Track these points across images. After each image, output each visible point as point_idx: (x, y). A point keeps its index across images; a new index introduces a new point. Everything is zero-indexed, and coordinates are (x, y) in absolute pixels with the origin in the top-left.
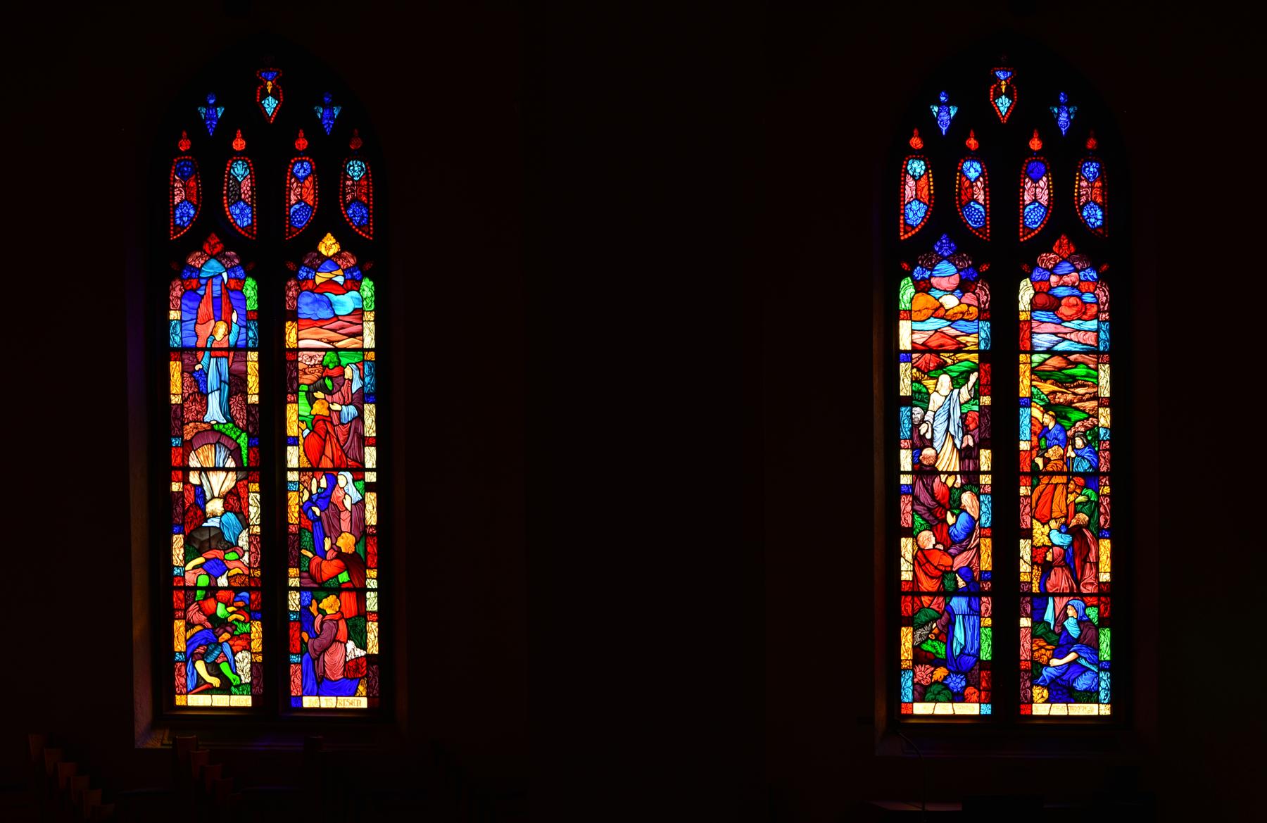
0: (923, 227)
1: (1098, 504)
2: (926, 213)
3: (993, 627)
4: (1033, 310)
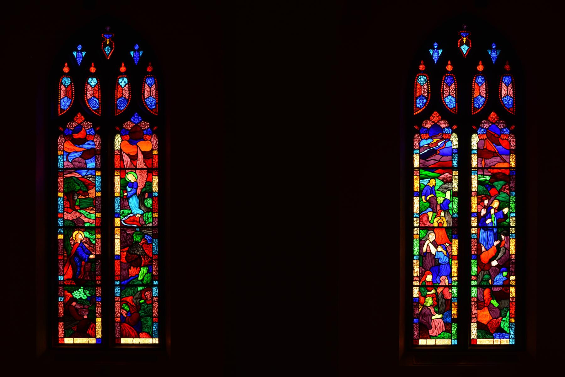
0: (69, 109)
2: (71, 103)
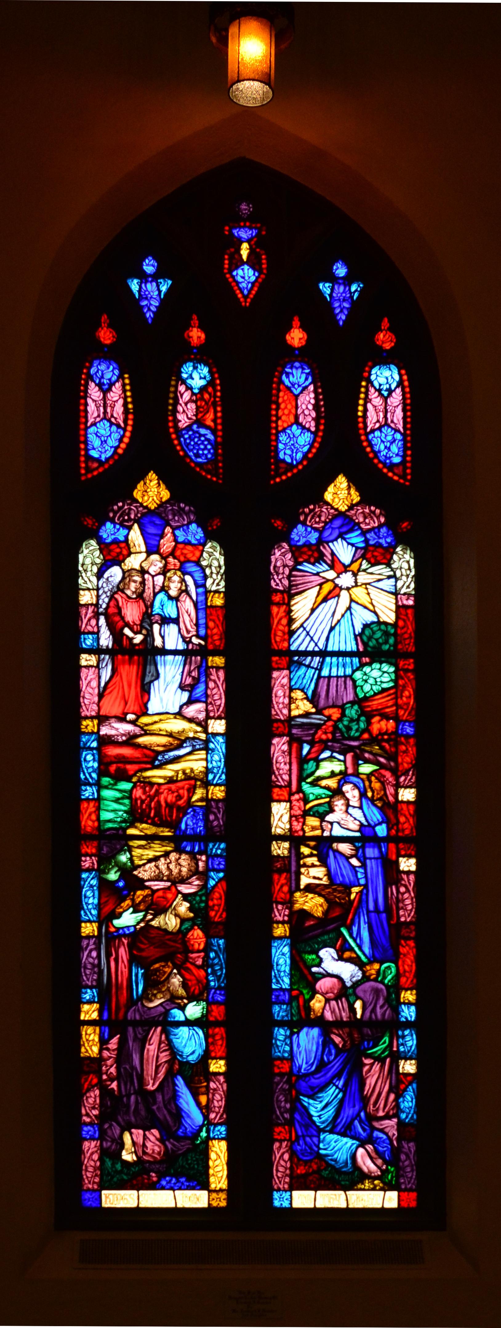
2: (121, 440)
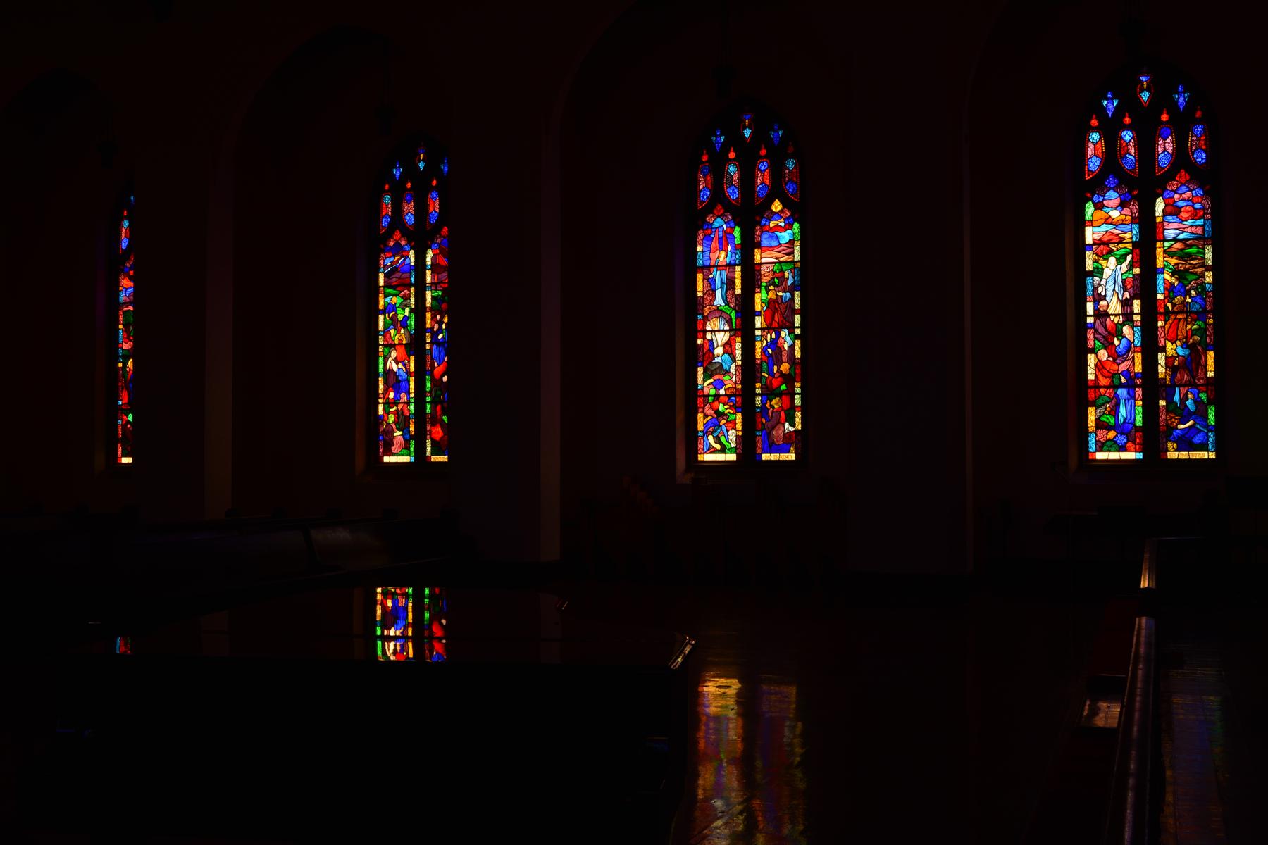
1: (1206, 330)
2: (1100, 163)
3: (1143, 406)
4: (1164, 216)
